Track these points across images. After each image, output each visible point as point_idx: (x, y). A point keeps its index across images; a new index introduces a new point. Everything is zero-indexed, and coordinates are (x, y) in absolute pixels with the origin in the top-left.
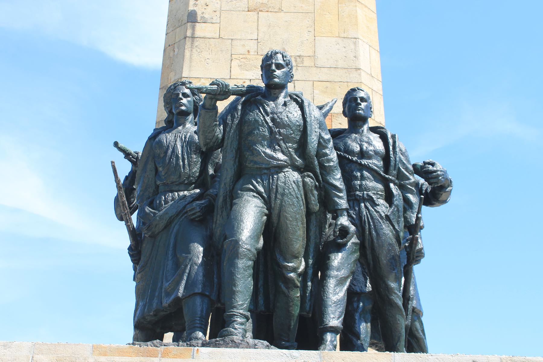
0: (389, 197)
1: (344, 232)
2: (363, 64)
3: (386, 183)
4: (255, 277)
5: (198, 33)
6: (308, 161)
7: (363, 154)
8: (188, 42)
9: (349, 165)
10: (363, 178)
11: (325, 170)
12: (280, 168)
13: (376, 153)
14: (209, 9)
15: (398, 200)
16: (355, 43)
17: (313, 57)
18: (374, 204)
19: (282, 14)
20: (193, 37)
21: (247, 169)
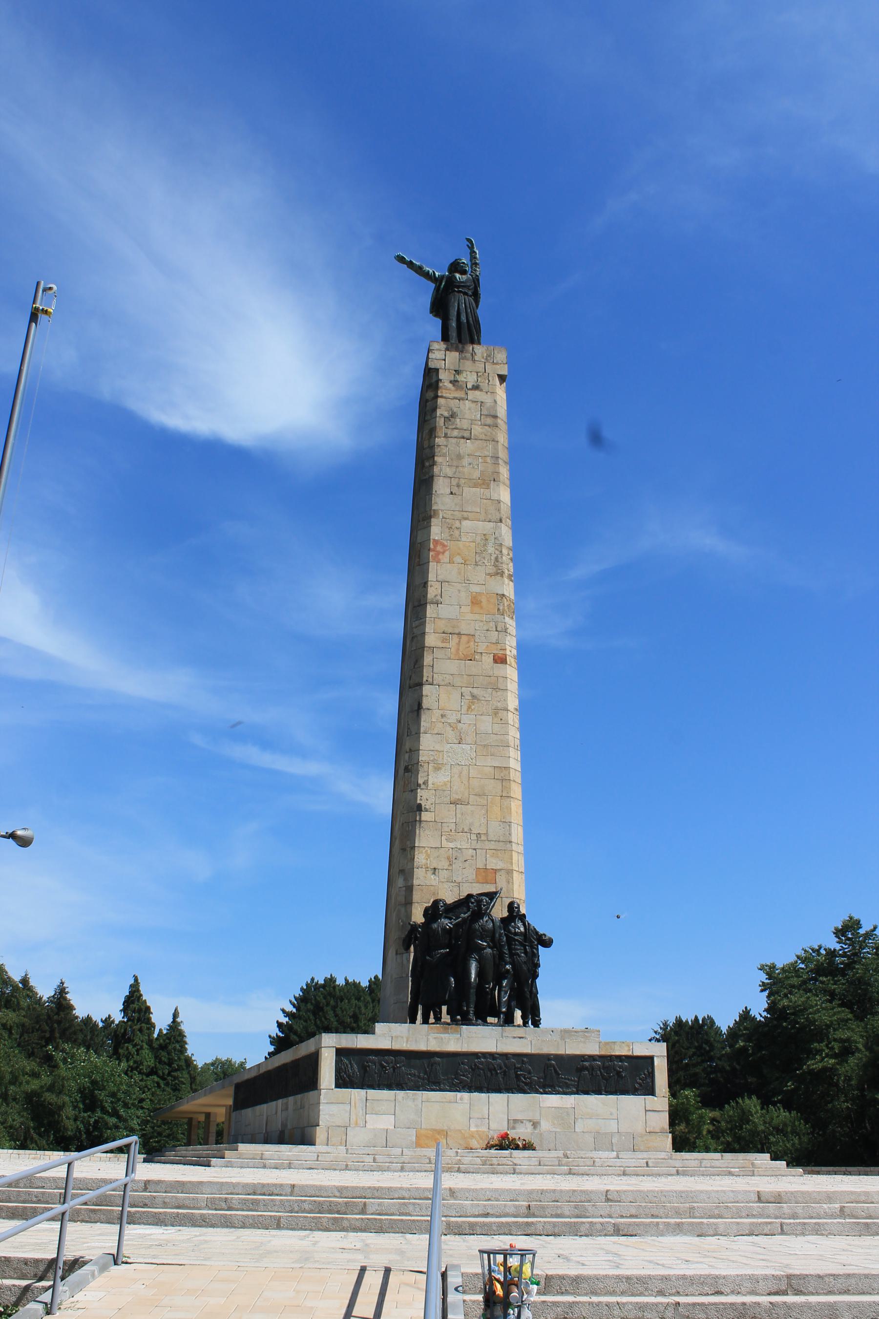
0: (526, 953)
1: (508, 970)
2: (514, 839)
3: (525, 946)
4: (476, 995)
5: (423, 818)
6: (495, 944)
7: (516, 934)
8: (418, 825)
9: (510, 941)
10: (515, 945)
11: (502, 946)
12: (485, 949)
13: (521, 932)
14: (429, 802)
15: (530, 955)
16: (510, 826)
17: (486, 834)
18: (520, 956)
19: (469, 806)
20: (420, 821)
21: (473, 949)
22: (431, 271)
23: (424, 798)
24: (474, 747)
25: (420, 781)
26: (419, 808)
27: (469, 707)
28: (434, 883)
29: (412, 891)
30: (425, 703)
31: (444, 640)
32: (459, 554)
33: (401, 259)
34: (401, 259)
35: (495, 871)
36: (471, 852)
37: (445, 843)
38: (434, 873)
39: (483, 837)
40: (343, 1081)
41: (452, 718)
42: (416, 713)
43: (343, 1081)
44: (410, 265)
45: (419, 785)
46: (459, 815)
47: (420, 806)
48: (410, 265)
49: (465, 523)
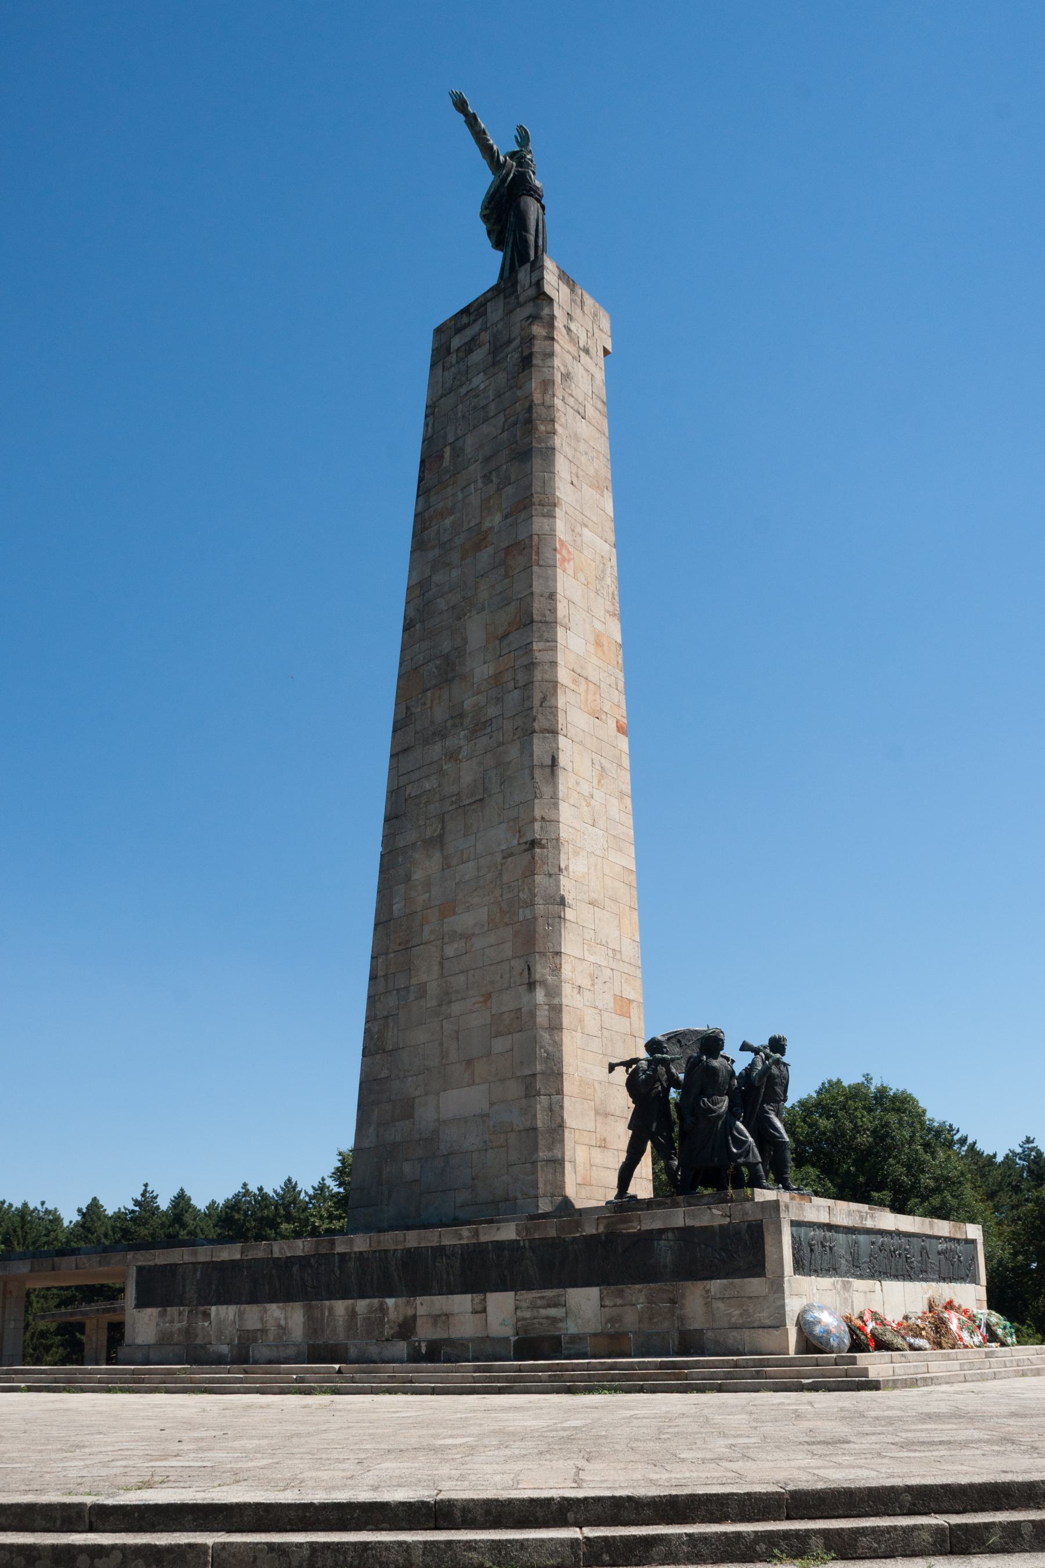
22: (495, 148)
23: (566, 888)
24: (606, 834)
25: (563, 866)
26: (562, 902)
27: (599, 781)
28: (580, 1006)
29: (560, 1011)
30: (563, 760)
31: (574, 681)
32: (582, 570)
33: (461, 105)
34: (461, 105)
35: (630, 1001)
36: (609, 971)
37: (587, 956)
38: (579, 993)
39: (618, 957)
40: (800, 1267)
41: (585, 788)
42: (548, 770)
43: (800, 1267)
44: (472, 121)
45: (560, 869)
46: (597, 922)
47: (563, 898)
48: (472, 121)
49: (585, 530)
